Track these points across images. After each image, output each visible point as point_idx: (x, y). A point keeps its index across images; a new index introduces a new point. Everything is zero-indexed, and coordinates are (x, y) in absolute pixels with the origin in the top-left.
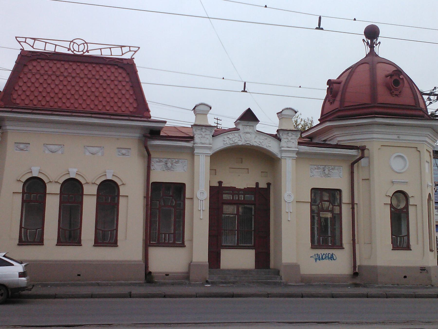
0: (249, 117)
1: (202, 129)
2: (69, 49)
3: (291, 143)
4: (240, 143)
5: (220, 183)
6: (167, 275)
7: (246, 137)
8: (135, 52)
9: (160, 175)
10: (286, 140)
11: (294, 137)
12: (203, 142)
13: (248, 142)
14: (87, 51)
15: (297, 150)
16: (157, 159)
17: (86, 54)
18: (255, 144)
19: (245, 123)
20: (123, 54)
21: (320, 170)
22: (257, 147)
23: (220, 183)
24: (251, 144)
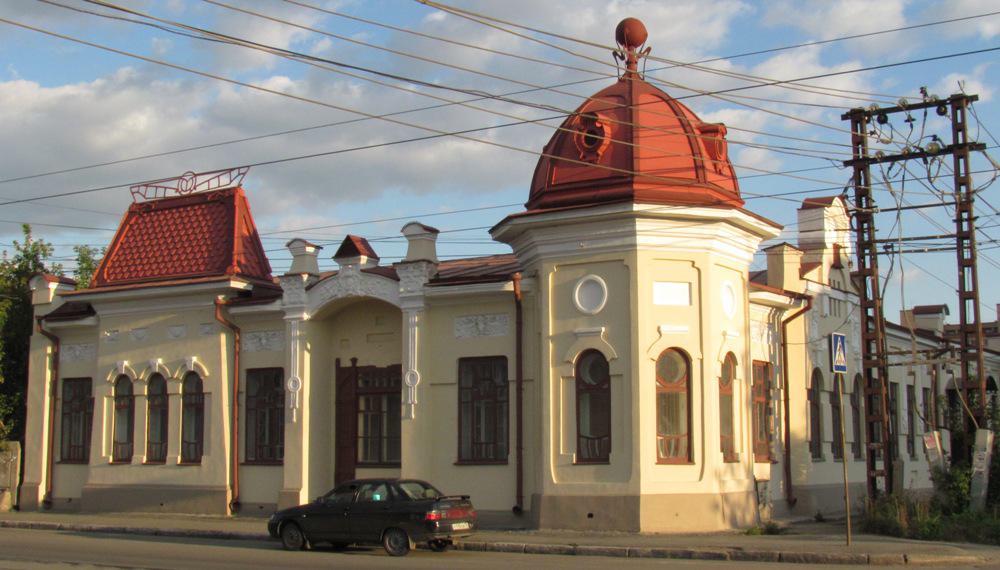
0: (349, 249)
1: (290, 280)
2: (177, 190)
3: (414, 284)
4: (340, 296)
5: (354, 360)
6: (261, 507)
7: (358, 285)
8: (244, 174)
9: (70, 370)
10: (407, 280)
11: (417, 273)
12: (292, 300)
13: (350, 292)
14: (195, 188)
15: (421, 294)
16: (251, 335)
17: (194, 192)
18: (361, 293)
19: (345, 260)
20: (231, 181)
21: (471, 325)
22: (365, 297)
23: (354, 360)
24: (354, 294)
